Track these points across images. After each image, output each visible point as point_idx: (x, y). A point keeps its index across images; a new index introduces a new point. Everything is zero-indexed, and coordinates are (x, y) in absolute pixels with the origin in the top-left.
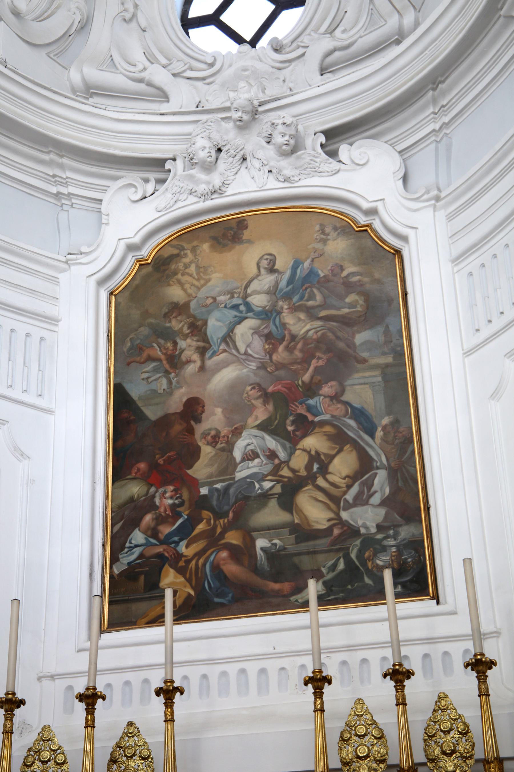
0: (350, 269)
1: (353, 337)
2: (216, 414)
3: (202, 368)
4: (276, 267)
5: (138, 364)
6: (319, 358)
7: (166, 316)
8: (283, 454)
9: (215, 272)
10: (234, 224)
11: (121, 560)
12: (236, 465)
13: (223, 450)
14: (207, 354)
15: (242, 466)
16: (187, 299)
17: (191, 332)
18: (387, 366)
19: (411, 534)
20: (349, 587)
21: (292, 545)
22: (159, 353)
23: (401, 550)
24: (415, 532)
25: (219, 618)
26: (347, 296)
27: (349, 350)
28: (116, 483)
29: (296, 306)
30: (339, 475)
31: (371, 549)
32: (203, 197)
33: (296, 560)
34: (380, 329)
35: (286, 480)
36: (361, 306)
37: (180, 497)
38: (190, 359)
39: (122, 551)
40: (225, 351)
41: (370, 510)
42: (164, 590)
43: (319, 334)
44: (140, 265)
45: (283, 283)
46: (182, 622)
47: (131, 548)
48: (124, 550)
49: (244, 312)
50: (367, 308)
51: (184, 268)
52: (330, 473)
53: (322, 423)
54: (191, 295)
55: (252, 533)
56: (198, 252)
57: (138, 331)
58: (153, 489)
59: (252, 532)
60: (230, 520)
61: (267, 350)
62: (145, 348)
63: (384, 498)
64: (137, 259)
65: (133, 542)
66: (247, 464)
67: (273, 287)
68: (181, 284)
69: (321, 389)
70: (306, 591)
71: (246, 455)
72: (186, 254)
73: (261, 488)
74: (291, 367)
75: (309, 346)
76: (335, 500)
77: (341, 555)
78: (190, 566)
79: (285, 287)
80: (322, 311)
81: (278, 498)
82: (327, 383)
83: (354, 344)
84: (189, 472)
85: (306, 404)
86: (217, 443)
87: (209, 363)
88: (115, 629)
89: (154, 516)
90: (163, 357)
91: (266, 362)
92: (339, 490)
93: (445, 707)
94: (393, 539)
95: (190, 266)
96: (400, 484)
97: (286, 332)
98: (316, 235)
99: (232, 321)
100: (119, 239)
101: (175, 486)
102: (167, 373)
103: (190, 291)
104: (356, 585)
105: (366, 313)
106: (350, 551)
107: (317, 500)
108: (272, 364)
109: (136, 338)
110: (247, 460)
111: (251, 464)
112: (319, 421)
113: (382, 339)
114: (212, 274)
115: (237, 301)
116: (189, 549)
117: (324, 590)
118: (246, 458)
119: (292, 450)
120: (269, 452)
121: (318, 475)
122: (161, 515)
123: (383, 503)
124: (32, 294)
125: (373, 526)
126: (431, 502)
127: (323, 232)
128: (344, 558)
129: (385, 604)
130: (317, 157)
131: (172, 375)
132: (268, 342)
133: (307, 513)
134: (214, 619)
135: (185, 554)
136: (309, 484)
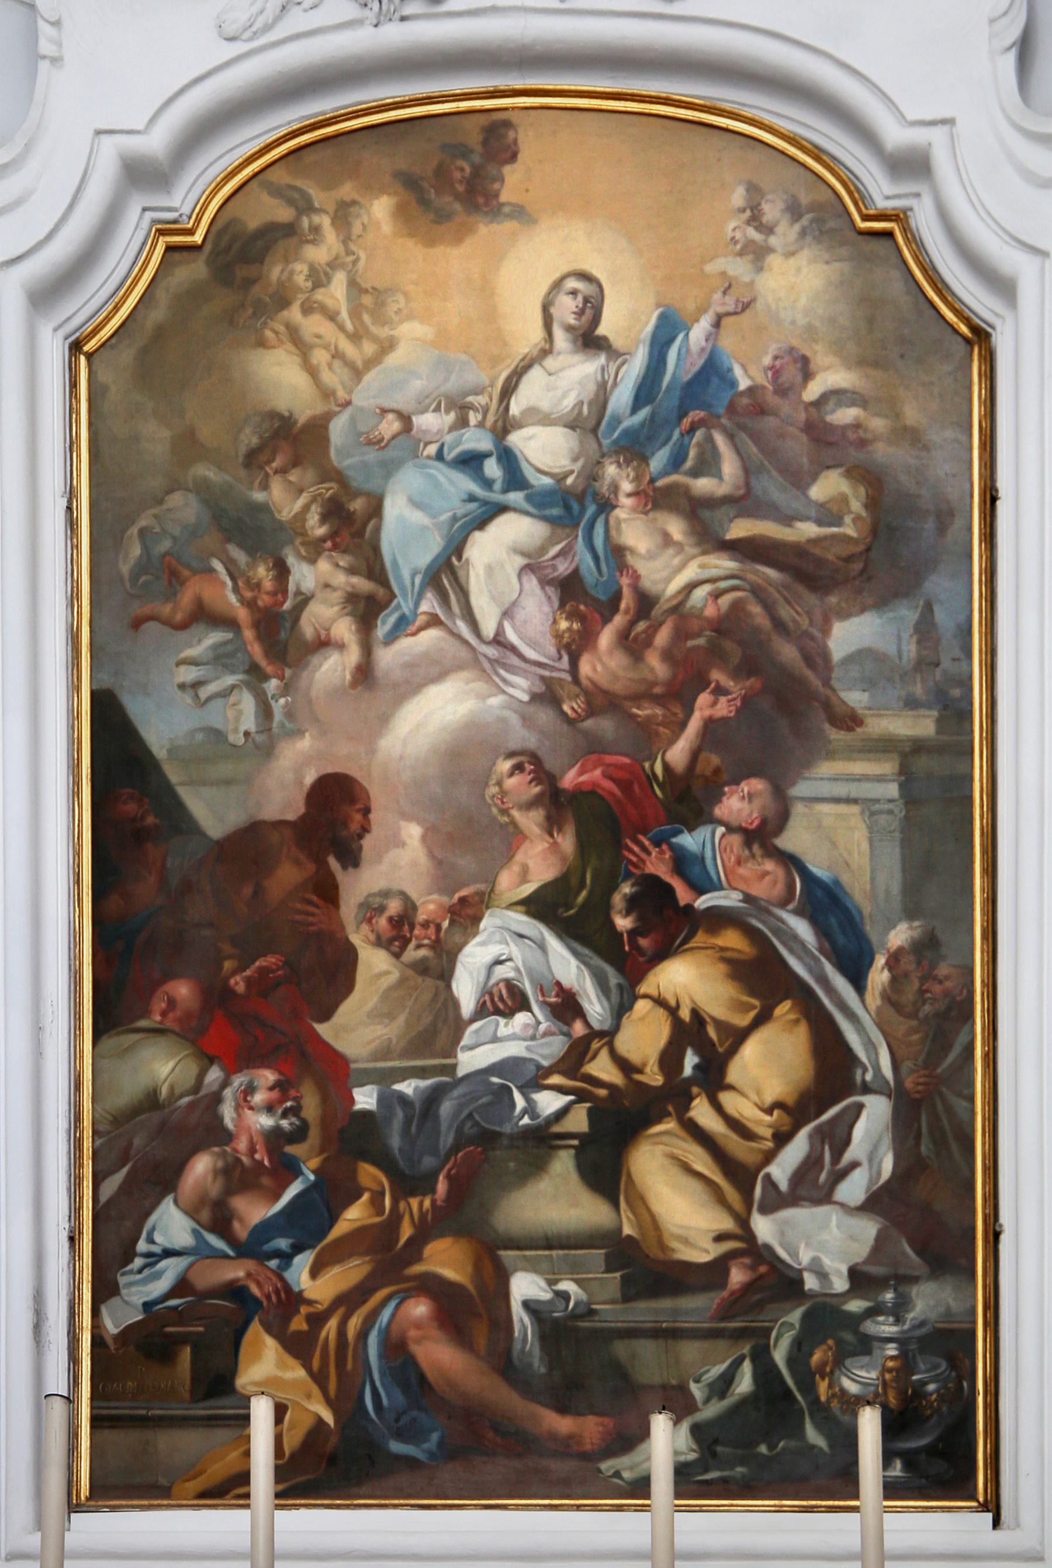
1: (826, 632)
2: (403, 844)
4: (602, 330)
5: (167, 630)
6: (720, 691)
7: (253, 459)
8: (598, 1008)
9: (410, 317)
10: (472, 134)
11: (124, 1292)
12: (459, 1026)
13: (421, 968)
14: (379, 623)
15: (477, 1031)
16: (320, 408)
17: (332, 535)
18: (918, 747)
19: (942, 1309)
20: (763, 1449)
21: (613, 1302)
22: (233, 598)
23: (910, 1354)
24: (953, 1304)
25: (402, 1502)
26: (814, 477)
27: (808, 673)
28: (104, 1038)
29: (660, 489)
30: (756, 1098)
31: (830, 1342)
33: (621, 1349)
34: (908, 614)
35: (602, 1092)
36: (857, 519)
37: (295, 1111)
38: (328, 635)
39: (126, 1265)
40: (434, 621)
41: (834, 1218)
42: (248, 1399)
43: (725, 601)
44: (170, 249)
45: (622, 397)
46: (298, 1502)
47: (153, 1258)
48: (132, 1261)
49: (498, 486)
50: (874, 532)
51: (309, 284)
52: (731, 1088)
54: (333, 393)
55: (502, 1253)
56: (357, 228)
57: (165, 507)
58: (214, 1074)
59: (499, 1249)
60: (439, 1203)
61: (562, 637)
62: (186, 573)
63: (875, 1187)
64: (160, 222)
65: (158, 1238)
66: (493, 1028)
67: (590, 404)
68: (302, 347)
69: (720, 801)
70: (643, 1446)
71: (491, 995)
72: (316, 229)
73: (531, 1109)
74: (635, 710)
75: (690, 643)
77: (746, 1350)
79: (628, 411)
80: (737, 520)
81: (579, 1151)
83: (826, 655)
84: (323, 1029)
85: (672, 847)
86: (405, 942)
87: (387, 658)
88: (111, 1503)
89: (220, 1164)
90: (242, 614)
91: (560, 679)
92: (753, 1144)
94: (891, 1319)
95: (329, 279)
97: (625, 581)
98: (732, 225)
99: (460, 512)
100: (99, 133)
101: (281, 1073)
102: (256, 674)
103: (328, 378)
104: (781, 1444)
105: (868, 550)
107: (688, 1169)
108: (577, 690)
109: (157, 530)
110: (493, 1014)
111: (506, 1027)
112: (709, 909)
113: (911, 649)
114: (401, 322)
115: (476, 440)
116: (319, 1282)
117: (694, 1451)
118: (489, 1004)
119: (625, 996)
120: (557, 996)
121: (695, 1090)
125: (838, 1272)
128: (753, 1361)
129: (855, 1509)
131: (272, 685)
132: (567, 607)
133: (657, 1207)
134: (387, 1502)
135: (309, 1295)
136: (669, 1114)
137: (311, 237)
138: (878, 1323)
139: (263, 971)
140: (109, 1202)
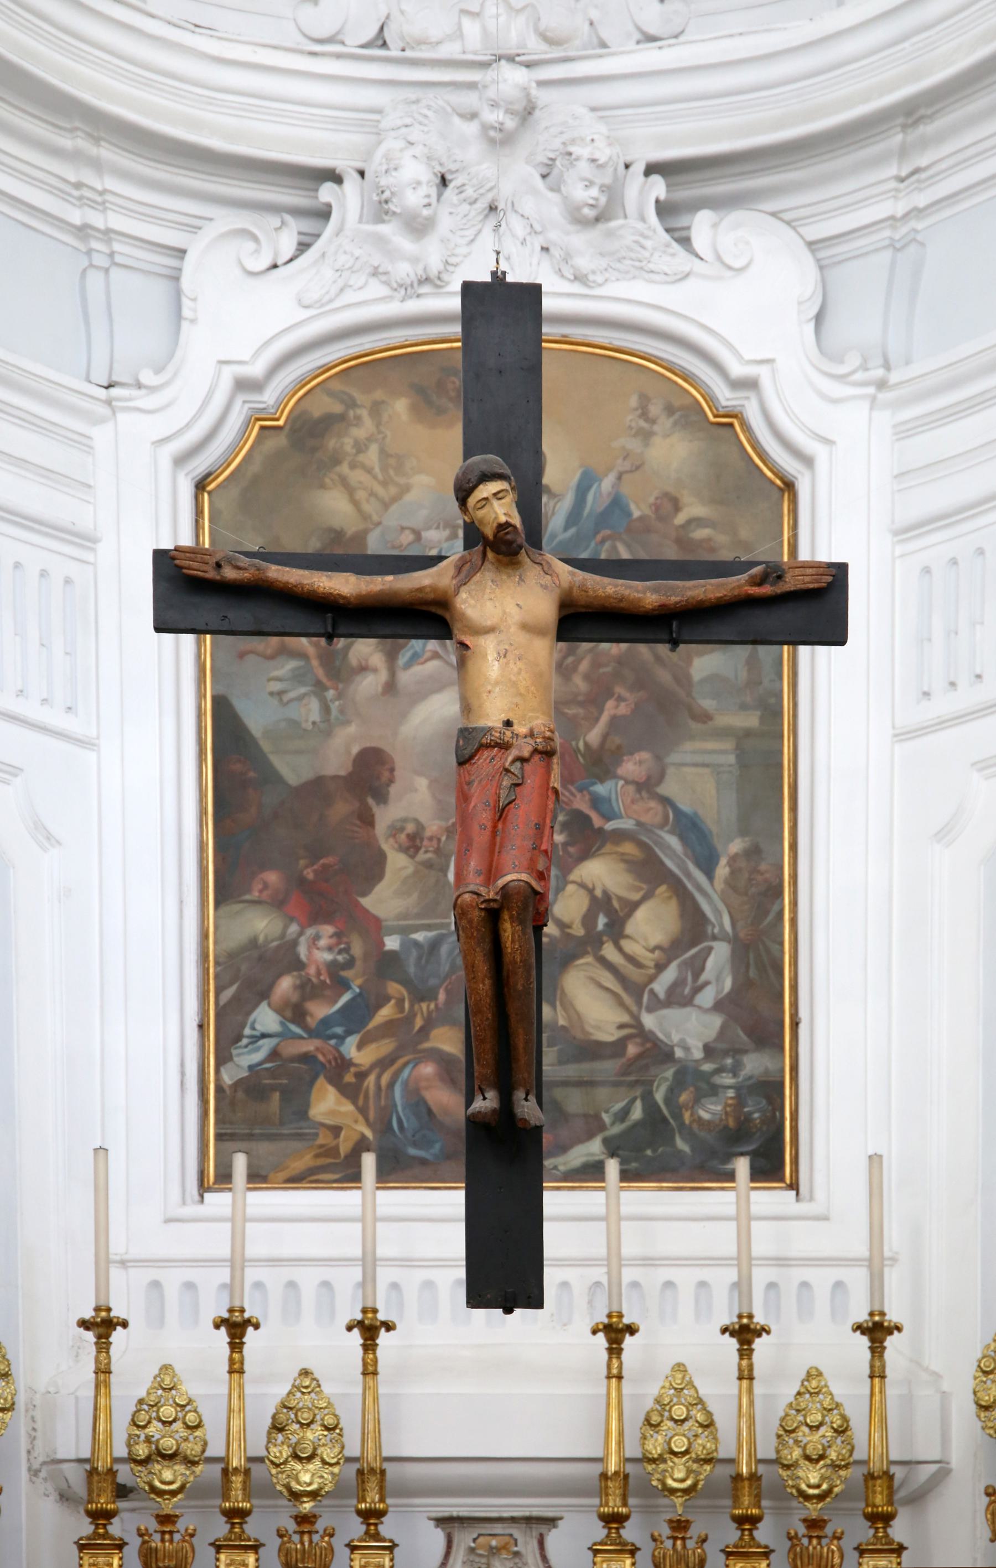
0: (693, 509)
2: (416, 790)
3: (391, 687)
6: (620, 699)
11: (235, 1059)
13: (428, 865)
14: (400, 656)
16: (361, 526)
20: (649, 1152)
30: (644, 944)
32: (403, 292)
40: (436, 655)
41: (694, 1017)
44: (263, 428)
51: (354, 451)
52: (628, 937)
53: (620, 836)
54: (370, 517)
56: (385, 417)
58: (294, 928)
60: (440, 1006)
65: (258, 1026)
72: (358, 418)
74: (567, 711)
75: (601, 670)
76: (636, 989)
78: (366, 1084)
82: (632, 754)
83: (688, 677)
84: (366, 902)
85: (590, 793)
86: (417, 849)
87: (406, 678)
89: (298, 982)
92: (643, 971)
93: (816, 1390)
95: (367, 447)
96: (752, 973)
98: (630, 417)
101: (336, 927)
102: (319, 687)
103: (367, 507)
104: (660, 1150)
106: (654, 1089)
113: (743, 675)
116: (363, 1052)
121: (605, 938)
122: (310, 980)
123: (718, 1006)
124: (48, 478)
126: (803, 1013)
127: (644, 415)
128: (643, 1100)
130: (646, 237)
131: (331, 694)
135: (356, 1061)
137: (355, 422)
138: (722, 1077)
139: (325, 867)
140: (225, 1005)
